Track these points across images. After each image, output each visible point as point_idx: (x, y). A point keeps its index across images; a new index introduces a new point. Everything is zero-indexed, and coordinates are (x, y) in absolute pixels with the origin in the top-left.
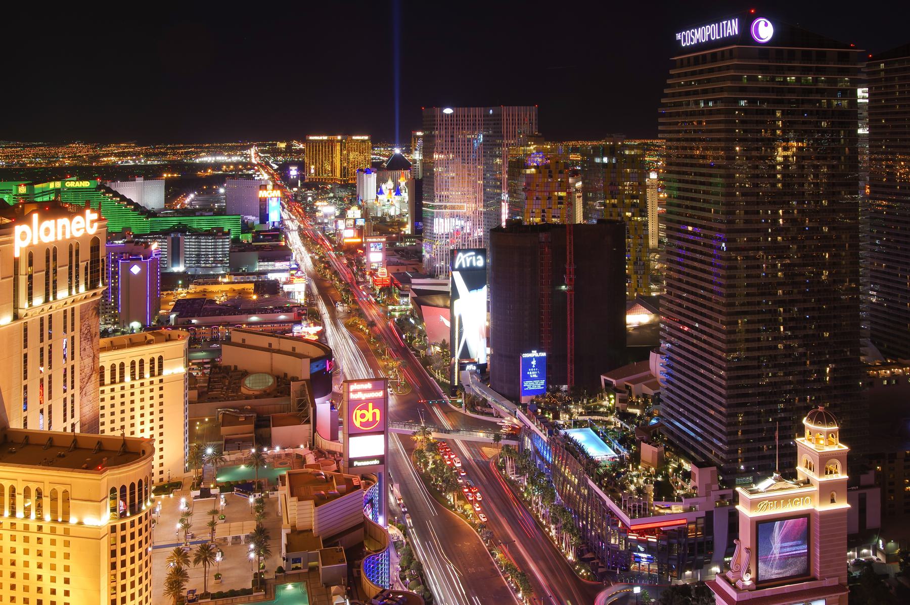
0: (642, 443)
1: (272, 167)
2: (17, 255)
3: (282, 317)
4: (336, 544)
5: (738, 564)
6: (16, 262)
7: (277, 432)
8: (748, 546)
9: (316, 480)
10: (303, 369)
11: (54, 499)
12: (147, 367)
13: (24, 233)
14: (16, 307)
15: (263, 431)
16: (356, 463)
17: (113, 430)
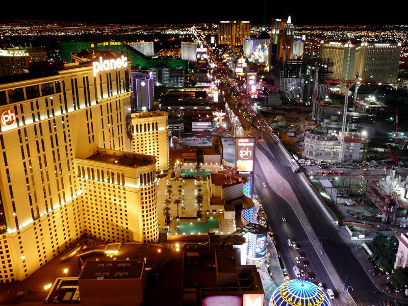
1: (202, 37)
2: (95, 75)
3: (208, 108)
4: (231, 204)
6: (95, 79)
7: (206, 157)
11: (118, 176)
12: (151, 126)
13: (97, 66)
14: (97, 98)
15: (200, 156)
16: (240, 173)
17: (138, 151)
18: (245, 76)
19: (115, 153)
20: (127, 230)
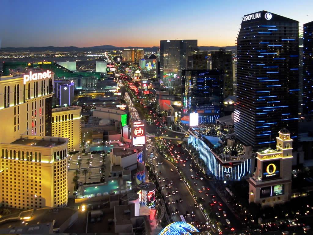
1: (111, 58)
2: (25, 83)
3: (113, 103)
4: (128, 169)
7: (110, 136)
9: (122, 150)
13: (27, 77)
14: (24, 99)
15: (105, 136)
18: (141, 82)
19: (35, 138)
20: (40, 198)
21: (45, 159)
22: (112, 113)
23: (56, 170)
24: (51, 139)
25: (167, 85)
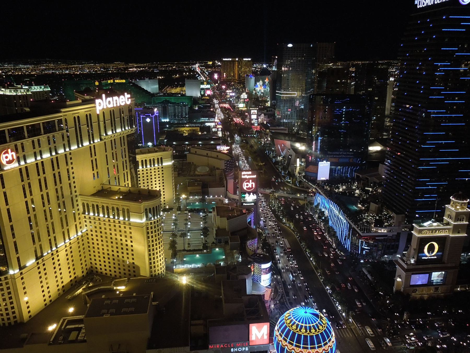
0: (371, 203)
2: (98, 113)
3: (212, 142)
5: (409, 254)
7: (211, 190)
8: (415, 247)
10: (221, 165)
11: (124, 212)
13: (100, 103)
14: (100, 135)
20: (134, 265)
21: (136, 217)
22: (211, 157)
23: (150, 232)
24: (139, 191)
25: (286, 117)
